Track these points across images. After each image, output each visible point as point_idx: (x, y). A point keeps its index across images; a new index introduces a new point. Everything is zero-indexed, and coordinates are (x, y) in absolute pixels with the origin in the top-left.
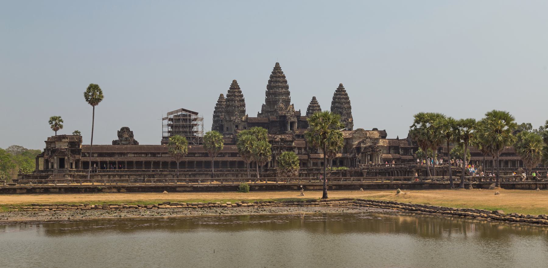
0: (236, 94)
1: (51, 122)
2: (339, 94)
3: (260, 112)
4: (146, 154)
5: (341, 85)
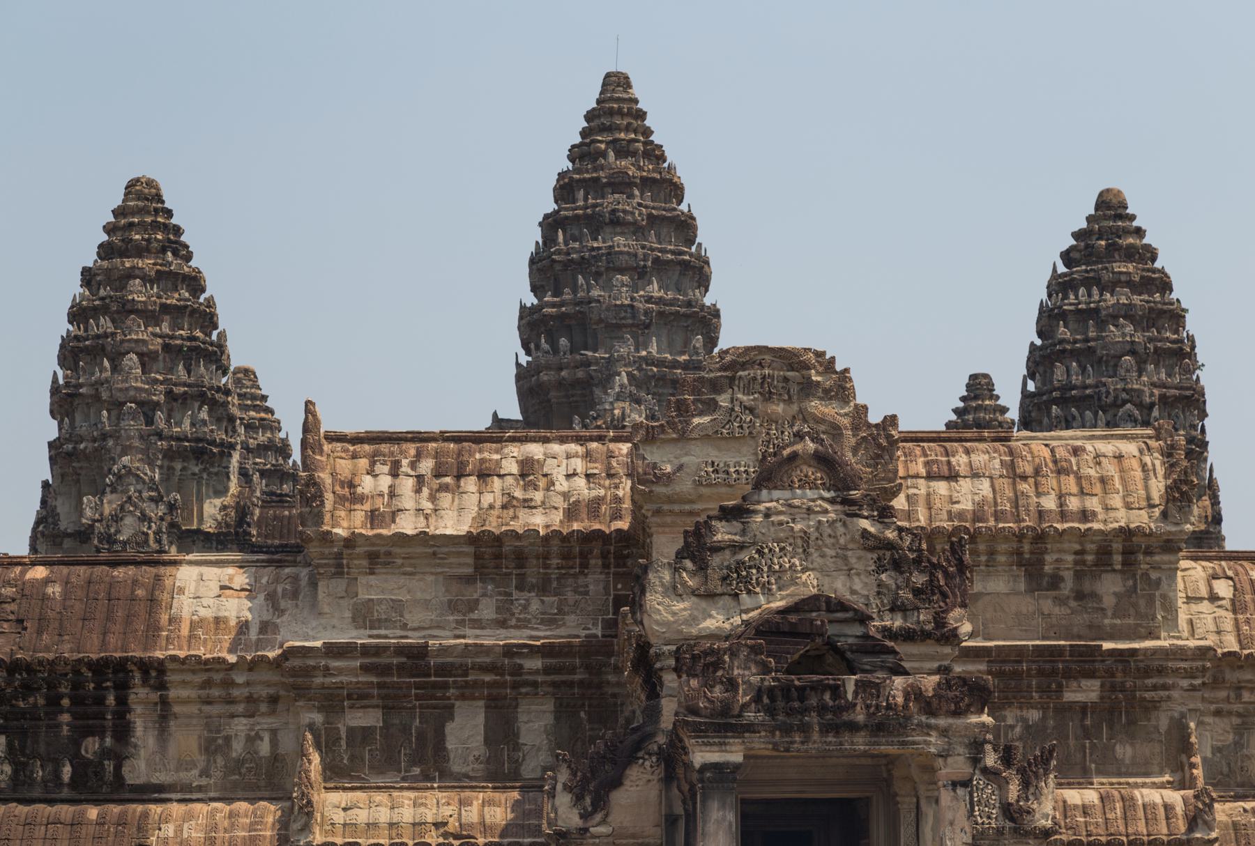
0: (138, 293)
2: (1088, 283)
5: (1110, 208)
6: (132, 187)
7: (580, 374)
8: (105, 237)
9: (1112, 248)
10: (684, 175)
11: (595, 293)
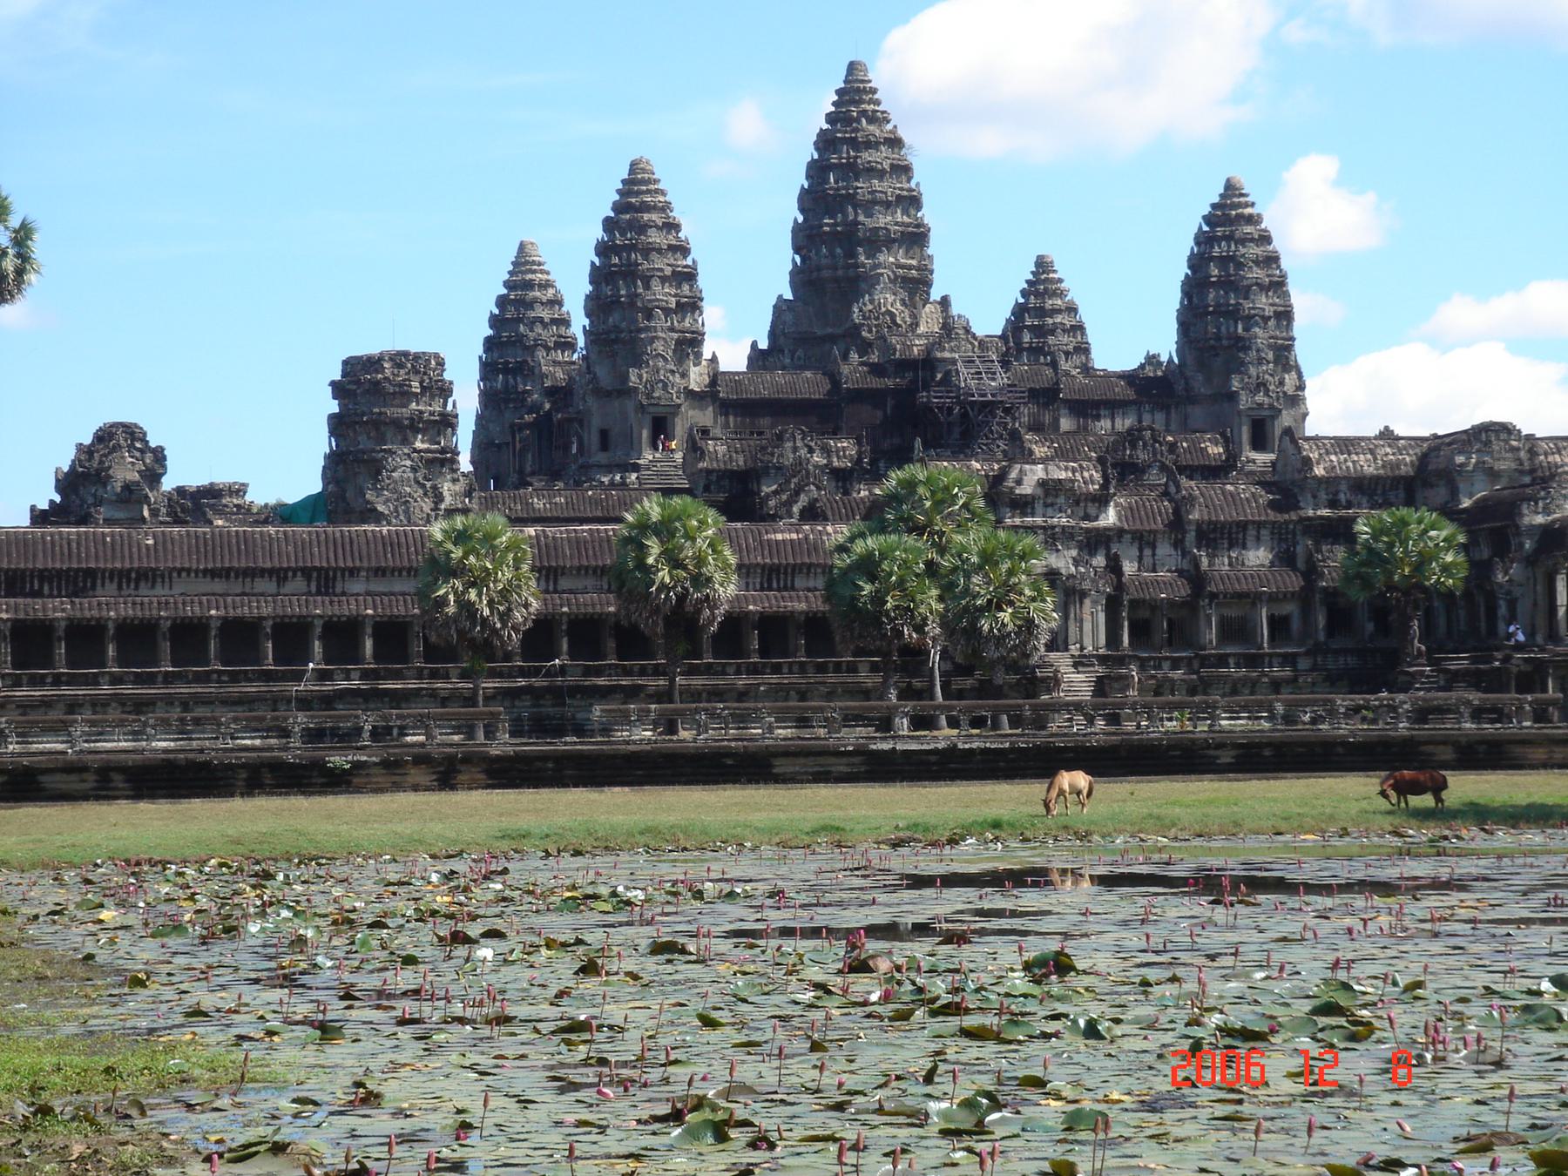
0: (655, 237)
1: (437, 356)
2: (1229, 238)
3: (763, 345)
4: (280, 575)
6: (634, 166)
7: (851, 272)
8: (617, 197)
9: (1240, 217)
10: (901, 133)
11: (861, 218)
